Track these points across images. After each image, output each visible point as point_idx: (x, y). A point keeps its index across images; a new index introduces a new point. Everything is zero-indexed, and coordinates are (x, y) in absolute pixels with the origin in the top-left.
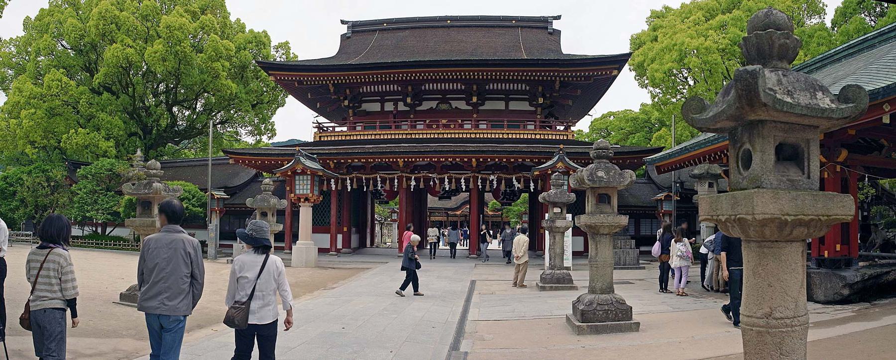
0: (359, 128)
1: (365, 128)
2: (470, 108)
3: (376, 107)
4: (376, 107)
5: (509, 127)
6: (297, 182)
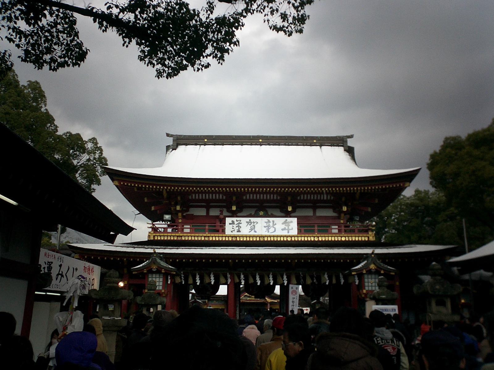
3: (202, 212)
5: (320, 231)
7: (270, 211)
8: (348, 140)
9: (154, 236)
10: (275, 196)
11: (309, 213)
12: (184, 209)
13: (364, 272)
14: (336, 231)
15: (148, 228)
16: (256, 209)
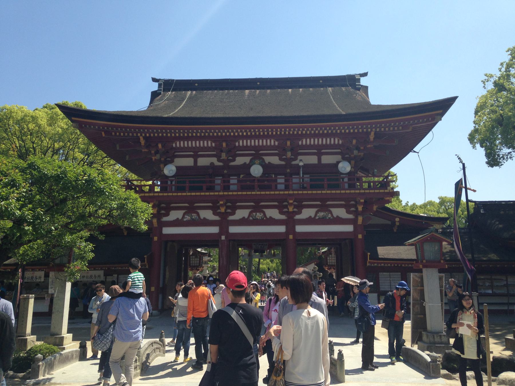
2: (283, 163)
10: (272, 141)
12: (168, 159)
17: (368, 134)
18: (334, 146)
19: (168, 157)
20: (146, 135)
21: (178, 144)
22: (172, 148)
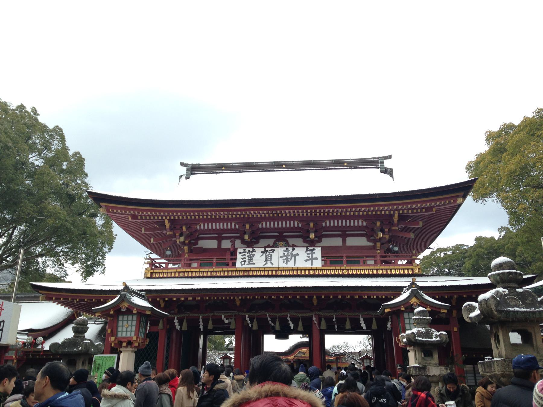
0: (195, 265)
1: (201, 265)
4: (212, 244)
5: (349, 263)
6: (120, 323)
7: (291, 241)
8: (385, 161)
9: (151, 274)
10: (296, 223)
11: (337, 242)
12: (193, 241)
13: (403, 309)
14: (372, 262)
15: (145, 263)
16: (274, 240)
17: (391, 216)
18: (358, 228)
19: (193, 240)
20: (170, 217)
21: (203, 226)
22: (196, 231)
